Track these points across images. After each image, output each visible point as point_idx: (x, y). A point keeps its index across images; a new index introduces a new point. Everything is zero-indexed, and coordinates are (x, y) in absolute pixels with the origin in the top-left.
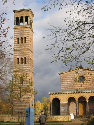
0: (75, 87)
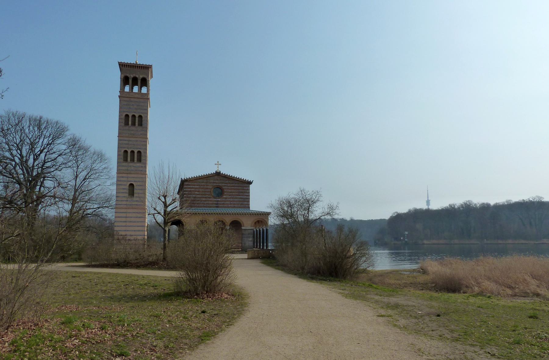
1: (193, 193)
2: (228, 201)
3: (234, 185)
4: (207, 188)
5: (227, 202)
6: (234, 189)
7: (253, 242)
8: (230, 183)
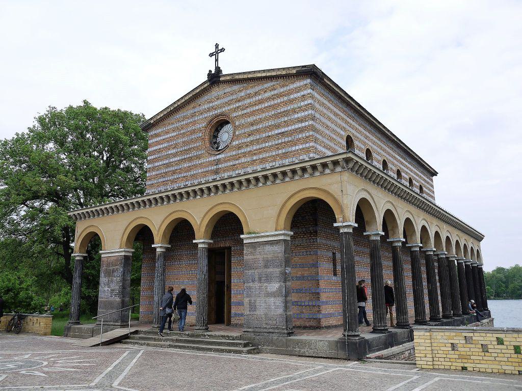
0: (192, 176)
1: (164, 153)
2: (244, 155)
3: (260, 97)
4: (193, 132)
5: (243, 160)
6: (262, 111)
8: (249, 96)
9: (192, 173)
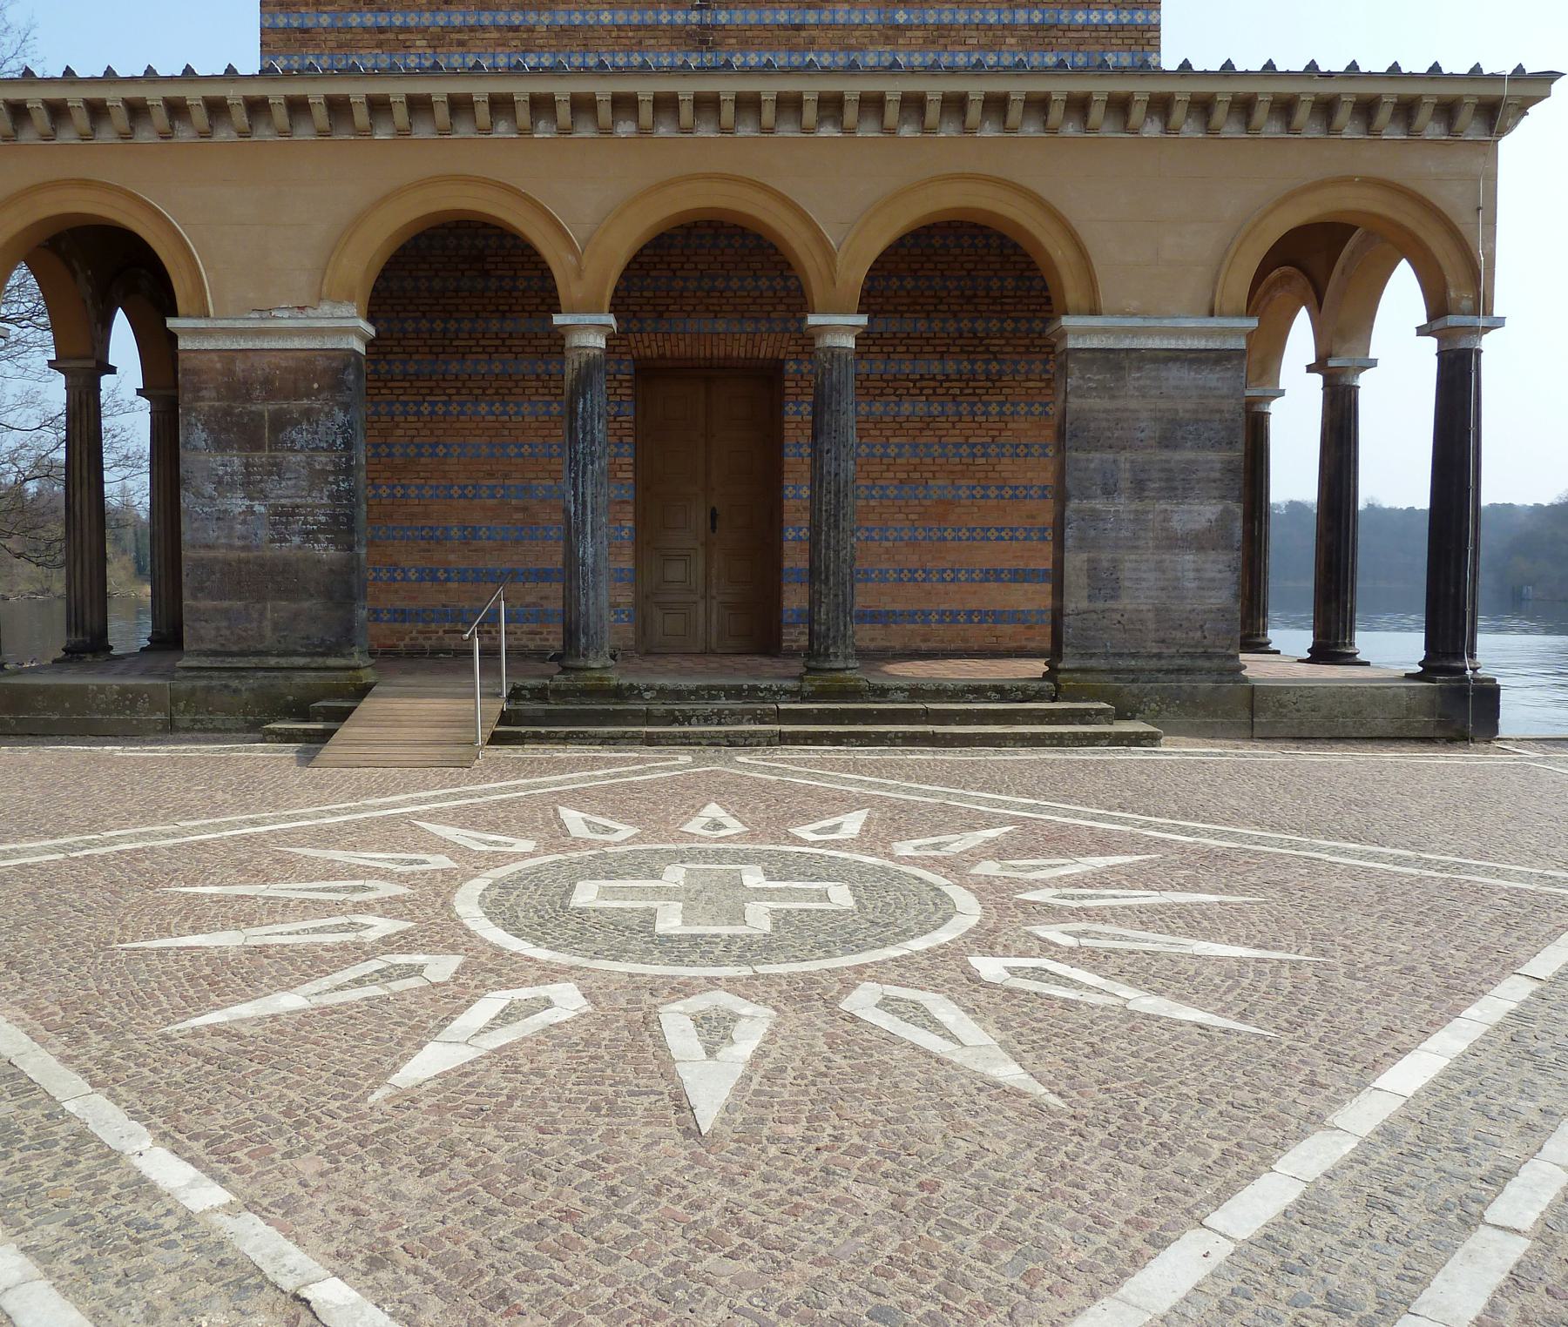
0: (566, 31)
7: (1235, 557)
9: (562, 19)
